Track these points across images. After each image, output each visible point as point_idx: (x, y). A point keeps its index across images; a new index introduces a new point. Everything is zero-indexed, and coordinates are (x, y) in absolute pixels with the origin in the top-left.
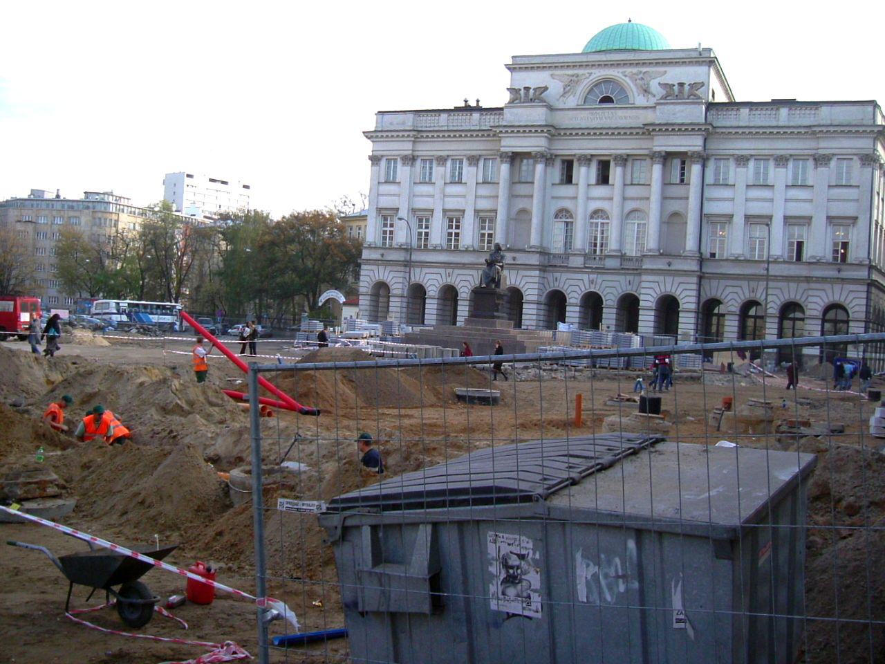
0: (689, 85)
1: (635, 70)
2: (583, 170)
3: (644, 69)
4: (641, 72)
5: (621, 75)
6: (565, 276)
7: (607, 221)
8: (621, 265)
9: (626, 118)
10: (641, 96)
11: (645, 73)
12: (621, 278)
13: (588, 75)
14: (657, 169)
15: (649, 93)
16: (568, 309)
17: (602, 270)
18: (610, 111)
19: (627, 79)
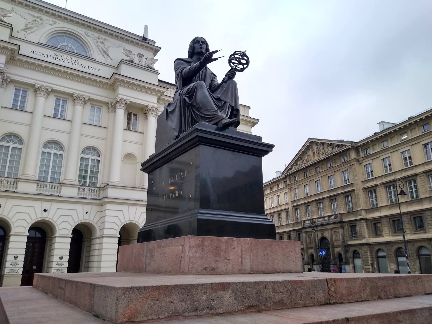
0: (146, 59)
1: (96, 35)
2: (41, 99)
3: (104, 37)
4: (102, 38)
5: (84, 34)
6: (11, 202)
7: (61, 153)
8: (78, 194)
9: (88, 68)
10: (101, 55)
11: (105, 39)
12: (79, 207)
13: (52, 23)
14: (121, 113)
15: (108, 55)
16: (12, 239)
17: (57, 198)
18: (74, 58)
19: (89, 38)
